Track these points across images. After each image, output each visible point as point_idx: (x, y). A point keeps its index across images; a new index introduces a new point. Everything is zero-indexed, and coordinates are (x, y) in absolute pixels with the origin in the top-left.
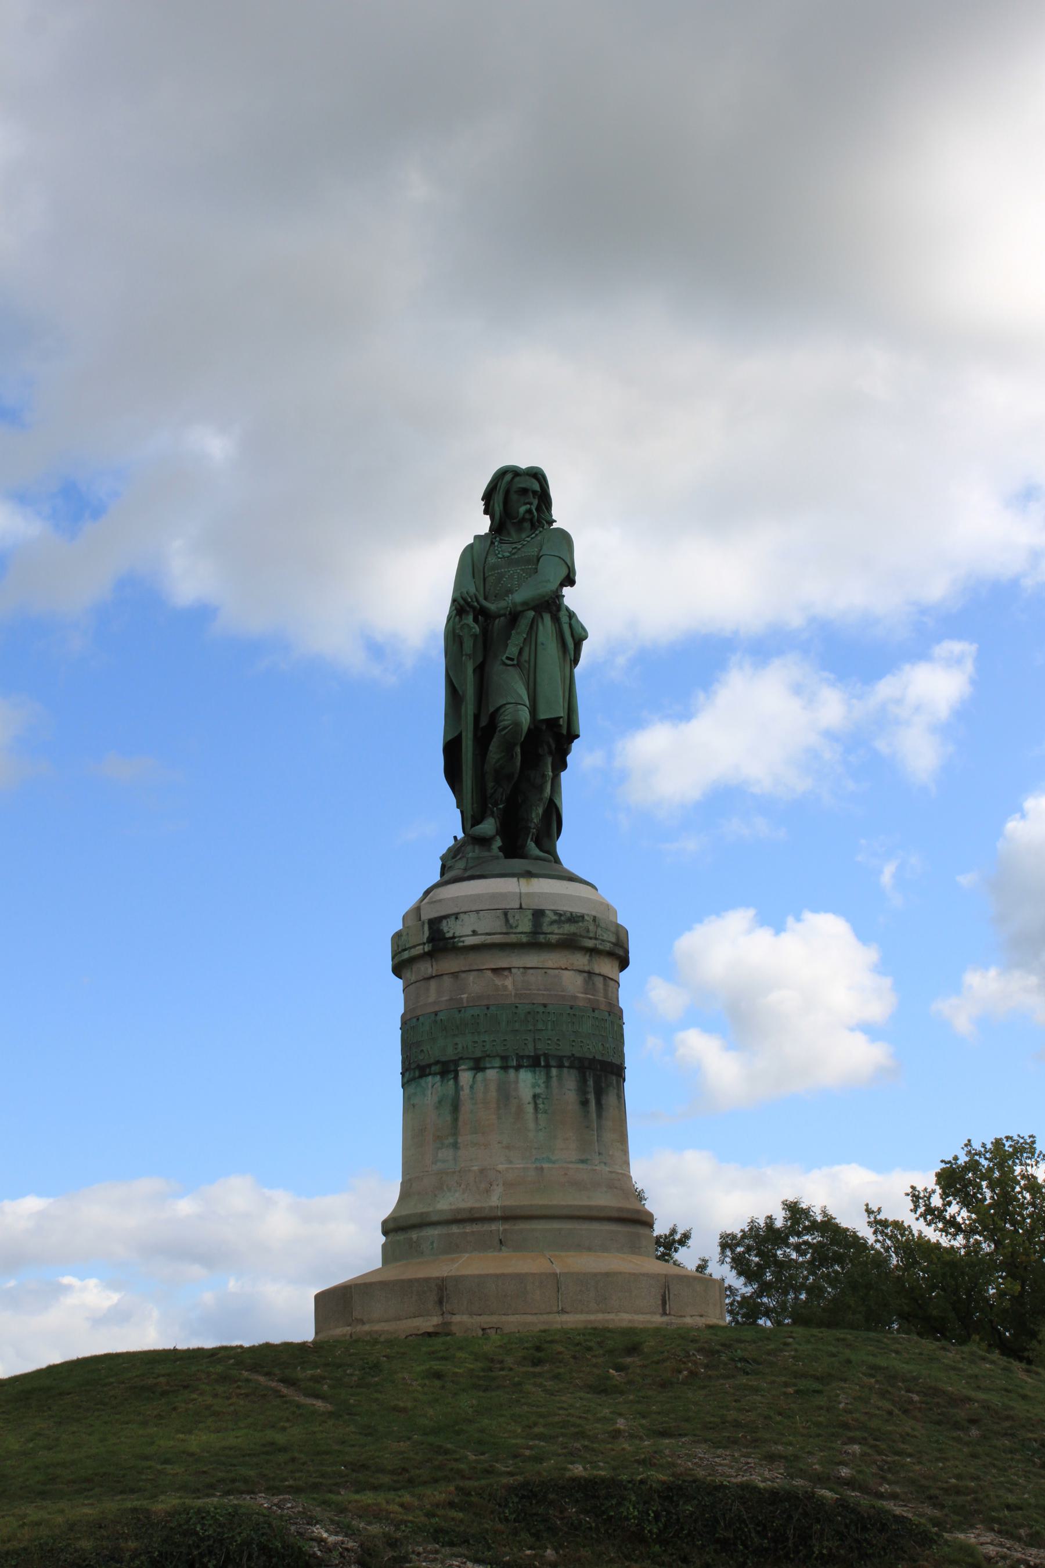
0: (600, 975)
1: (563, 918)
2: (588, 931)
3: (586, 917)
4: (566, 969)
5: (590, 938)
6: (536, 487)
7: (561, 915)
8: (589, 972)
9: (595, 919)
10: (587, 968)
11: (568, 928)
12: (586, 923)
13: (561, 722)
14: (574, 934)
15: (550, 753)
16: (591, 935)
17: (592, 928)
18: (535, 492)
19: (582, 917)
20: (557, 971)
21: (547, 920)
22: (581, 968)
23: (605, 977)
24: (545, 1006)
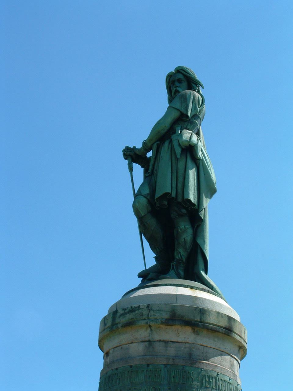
0: (160, 341)
1: (126, 311)
2: (142, 315)
3: (141, 307)
4: (132, 343)
5: (145, 319)
6: (180, 76)
7: (125, 309)
8: (149, 341)
9: (148, 306)
10: (147, 339)
11: (129, 316)
12: (140, 311)
13: (174, 195)
14: (132, 319)
15: (181, 216)
16: (144, 317)
17: (145, 312)
18: (180, 81)
19: (139, 307)
20: (128, 345)
21: (118, 314)
22: (143, 339)
23: (166, 342)
24: (117, 369)
